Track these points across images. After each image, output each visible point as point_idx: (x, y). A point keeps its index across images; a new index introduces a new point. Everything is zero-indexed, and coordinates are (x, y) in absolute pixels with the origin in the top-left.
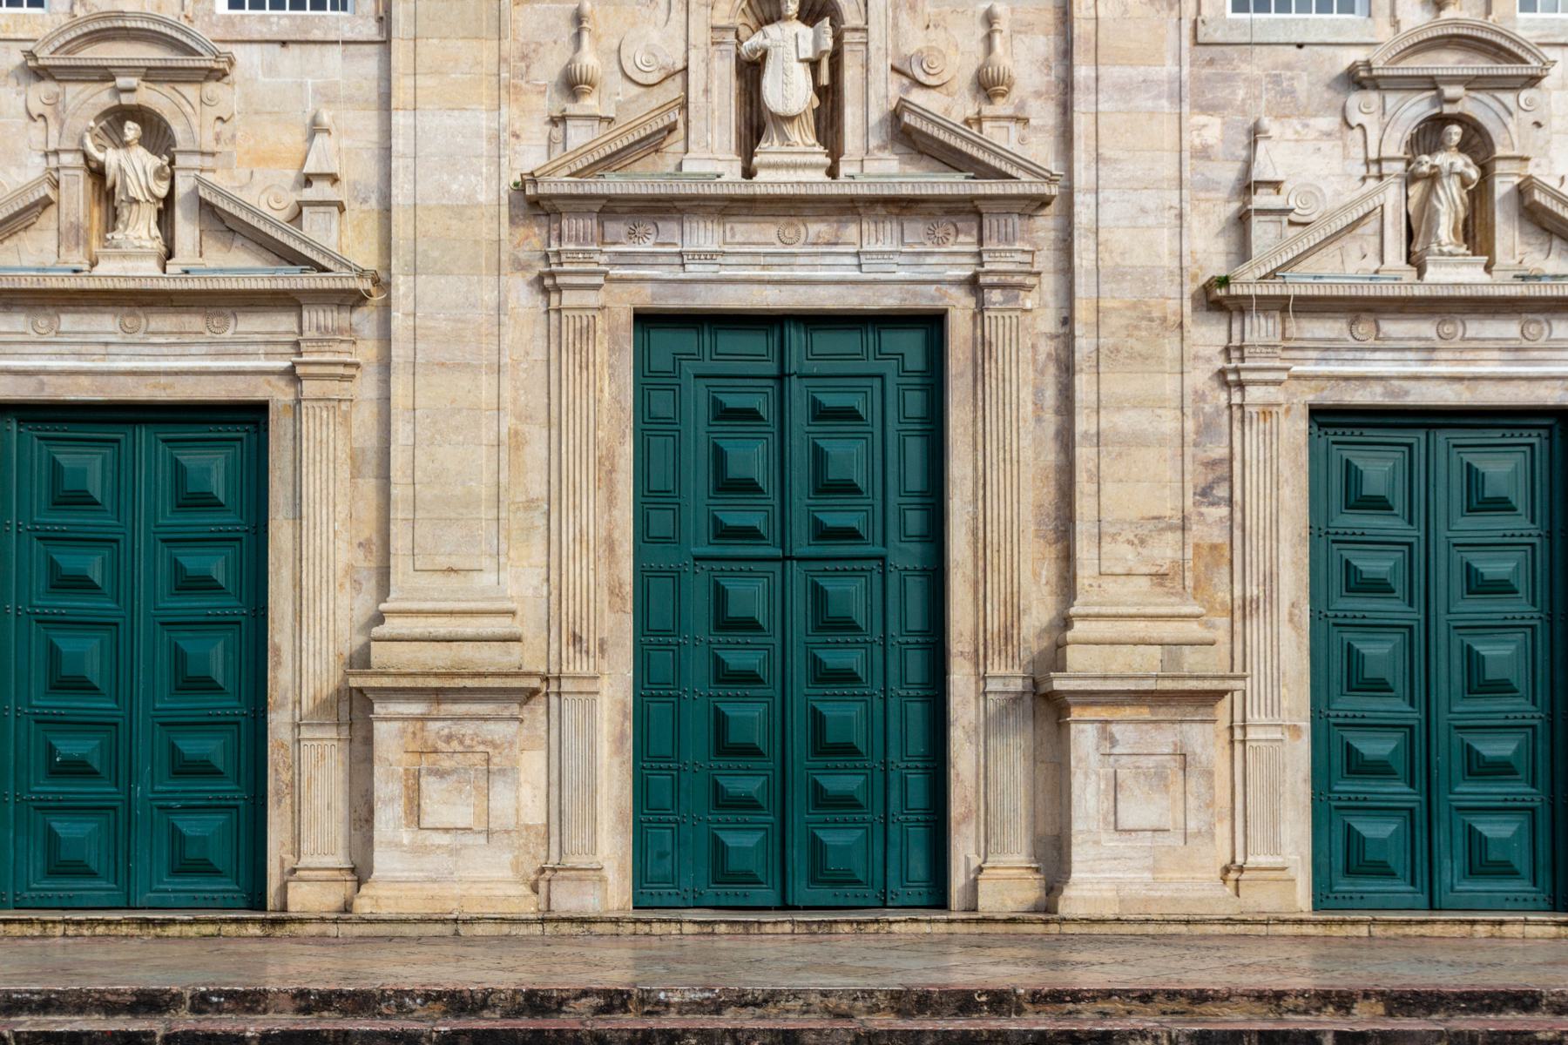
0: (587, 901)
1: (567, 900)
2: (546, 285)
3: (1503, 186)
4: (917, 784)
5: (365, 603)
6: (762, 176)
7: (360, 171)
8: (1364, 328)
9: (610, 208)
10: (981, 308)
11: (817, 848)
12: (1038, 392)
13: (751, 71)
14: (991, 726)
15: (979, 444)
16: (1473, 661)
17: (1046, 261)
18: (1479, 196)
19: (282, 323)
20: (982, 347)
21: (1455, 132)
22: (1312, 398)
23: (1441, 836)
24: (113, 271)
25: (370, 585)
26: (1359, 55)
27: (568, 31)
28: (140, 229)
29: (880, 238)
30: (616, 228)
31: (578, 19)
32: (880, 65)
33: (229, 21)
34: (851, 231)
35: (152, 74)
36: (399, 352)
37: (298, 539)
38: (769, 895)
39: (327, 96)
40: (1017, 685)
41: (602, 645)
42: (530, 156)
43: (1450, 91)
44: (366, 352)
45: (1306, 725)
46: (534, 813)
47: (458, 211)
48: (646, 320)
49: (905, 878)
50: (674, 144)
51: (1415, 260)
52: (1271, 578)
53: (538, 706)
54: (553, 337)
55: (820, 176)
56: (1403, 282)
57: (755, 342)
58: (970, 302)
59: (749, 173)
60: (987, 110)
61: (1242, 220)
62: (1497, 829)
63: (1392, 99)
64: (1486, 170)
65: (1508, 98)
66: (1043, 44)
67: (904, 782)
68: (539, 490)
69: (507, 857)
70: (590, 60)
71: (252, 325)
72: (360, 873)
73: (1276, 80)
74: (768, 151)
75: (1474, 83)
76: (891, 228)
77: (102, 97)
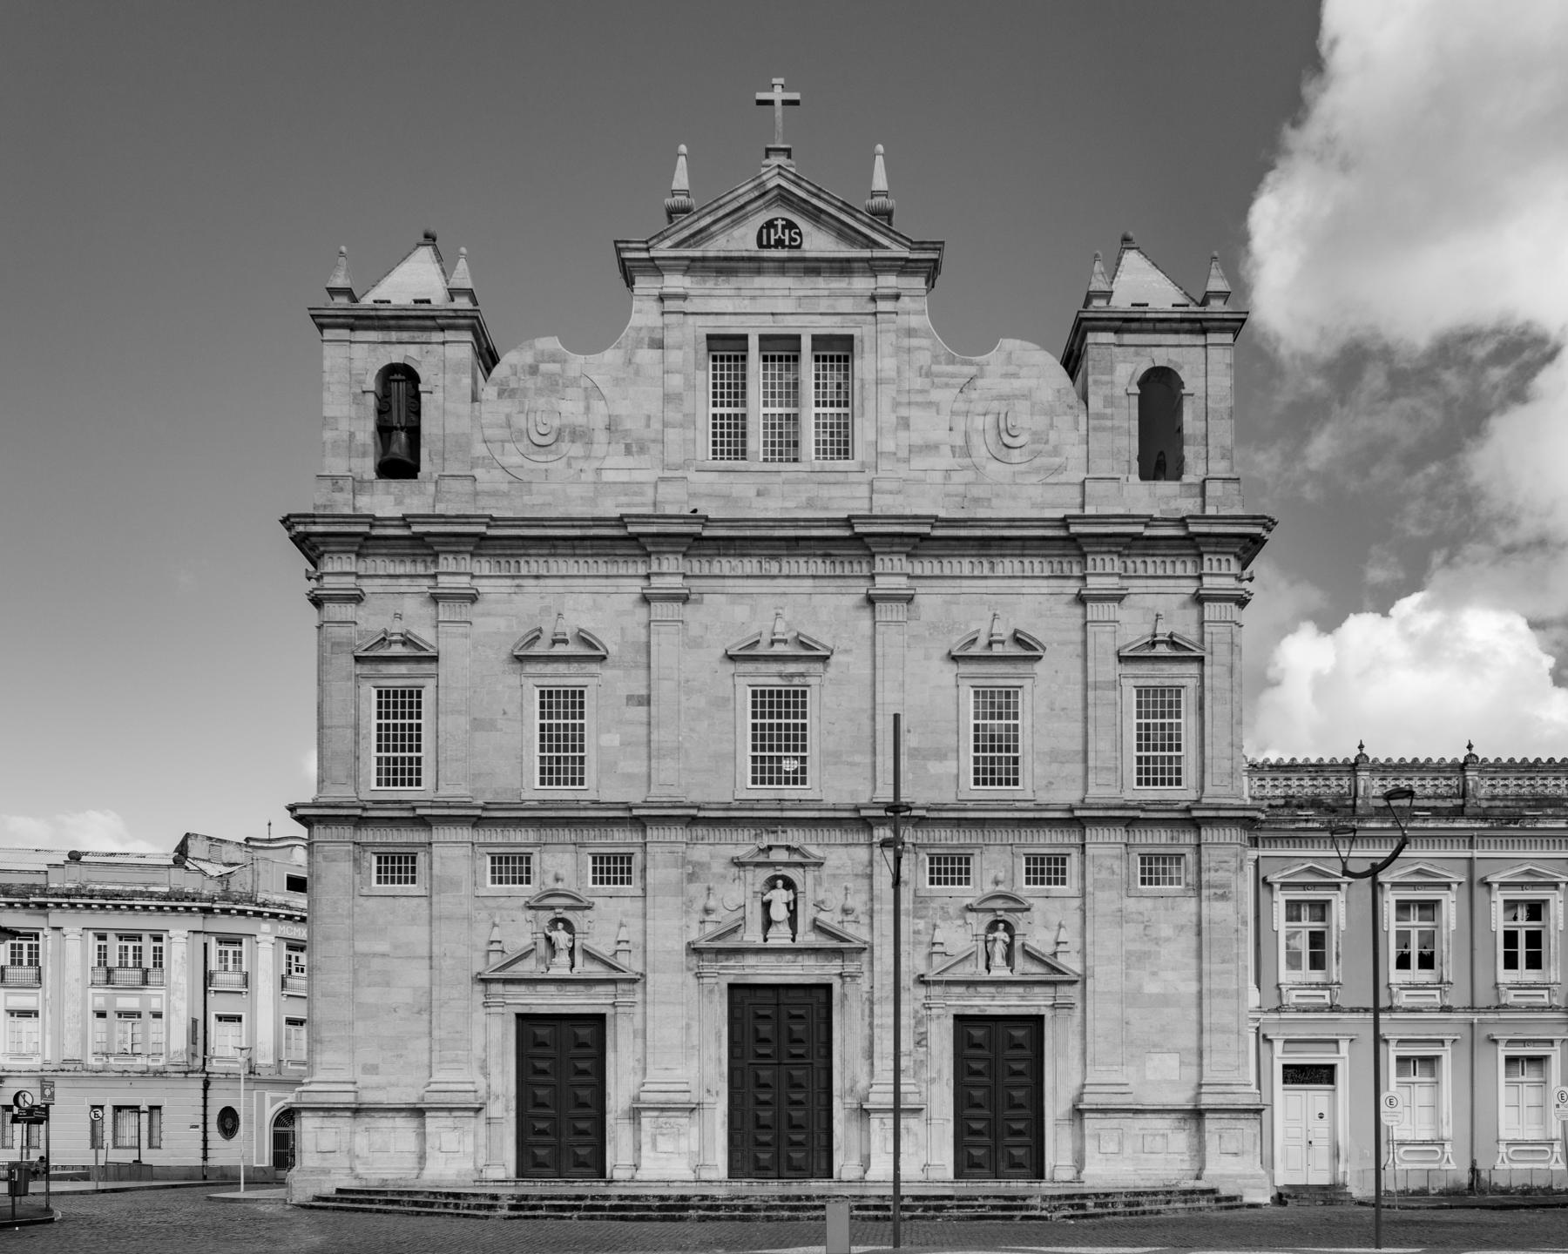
0: (712, 1175)
1: (705, 1175)
2: (699, 976)
3: (1017, 944)
4: (823, 1137)
5: (638, 1079)
6: (769, 941)
7: (637, 938)
8: (971, 990)
9: (719, 951)
10: (844, 983)
11: (789, 1159)
12: (863, 1011)
13: (767, 905)
14: (848, 1119)
15: (843, 1026)
16: (1011, 1097)
17: (865, 968)
18: (1010, 947)
19: (611, 988)
20: (844, 996)
21: (1001, 926)
22: (954, 1012)
23: (999, 1155)
24: (554, 973)
25: (640, 1073)
26: (968, 901)
27: (705, 893)
28: (563, 958)
29: (809, 961)
30: (720, 957)
31: (709, 889)
32: (810, 904)
33: (592, 889)
34: (800, 958)
35: (567, 908)
36: (649, 998)
37: (616, 1058)
38: (770, 1173)
39: (625, 914)
40: (855, 1106)
41: (717, 1093)
42: (694, 935)
43: (999, 913)
44: (638, 997)
45: (952, 1119)
46: (695, 1148)
47: (669, 953)
48: (731, 987)
49: (819, 1169)
50: (741, 930)
51: (988, 968)
52: (939, 1071)
53: (696, 1113)
54: (701, 992)
55: (790, 941)
56: (985, 976)
57: (769, 993)
58: (840, 981)
59: (766, 940)
60: (846, 919)
61: (931, 954)
62: (1017, 1152)
63: (980, 915)
64: (1012, 937)
65: (1019, 915)
66: (865, 897)
67: (819, 1138)
68: (696, 1043)
69: (686, 1161)
70: (712, 903)
71: (600, 989)
72: (636, 1167)
73: (942, 908)
74: (773, 931)
75: (1006, 910)
76: (813, 957)
77: (551, 915)
